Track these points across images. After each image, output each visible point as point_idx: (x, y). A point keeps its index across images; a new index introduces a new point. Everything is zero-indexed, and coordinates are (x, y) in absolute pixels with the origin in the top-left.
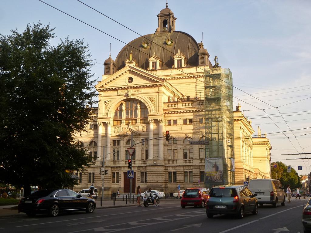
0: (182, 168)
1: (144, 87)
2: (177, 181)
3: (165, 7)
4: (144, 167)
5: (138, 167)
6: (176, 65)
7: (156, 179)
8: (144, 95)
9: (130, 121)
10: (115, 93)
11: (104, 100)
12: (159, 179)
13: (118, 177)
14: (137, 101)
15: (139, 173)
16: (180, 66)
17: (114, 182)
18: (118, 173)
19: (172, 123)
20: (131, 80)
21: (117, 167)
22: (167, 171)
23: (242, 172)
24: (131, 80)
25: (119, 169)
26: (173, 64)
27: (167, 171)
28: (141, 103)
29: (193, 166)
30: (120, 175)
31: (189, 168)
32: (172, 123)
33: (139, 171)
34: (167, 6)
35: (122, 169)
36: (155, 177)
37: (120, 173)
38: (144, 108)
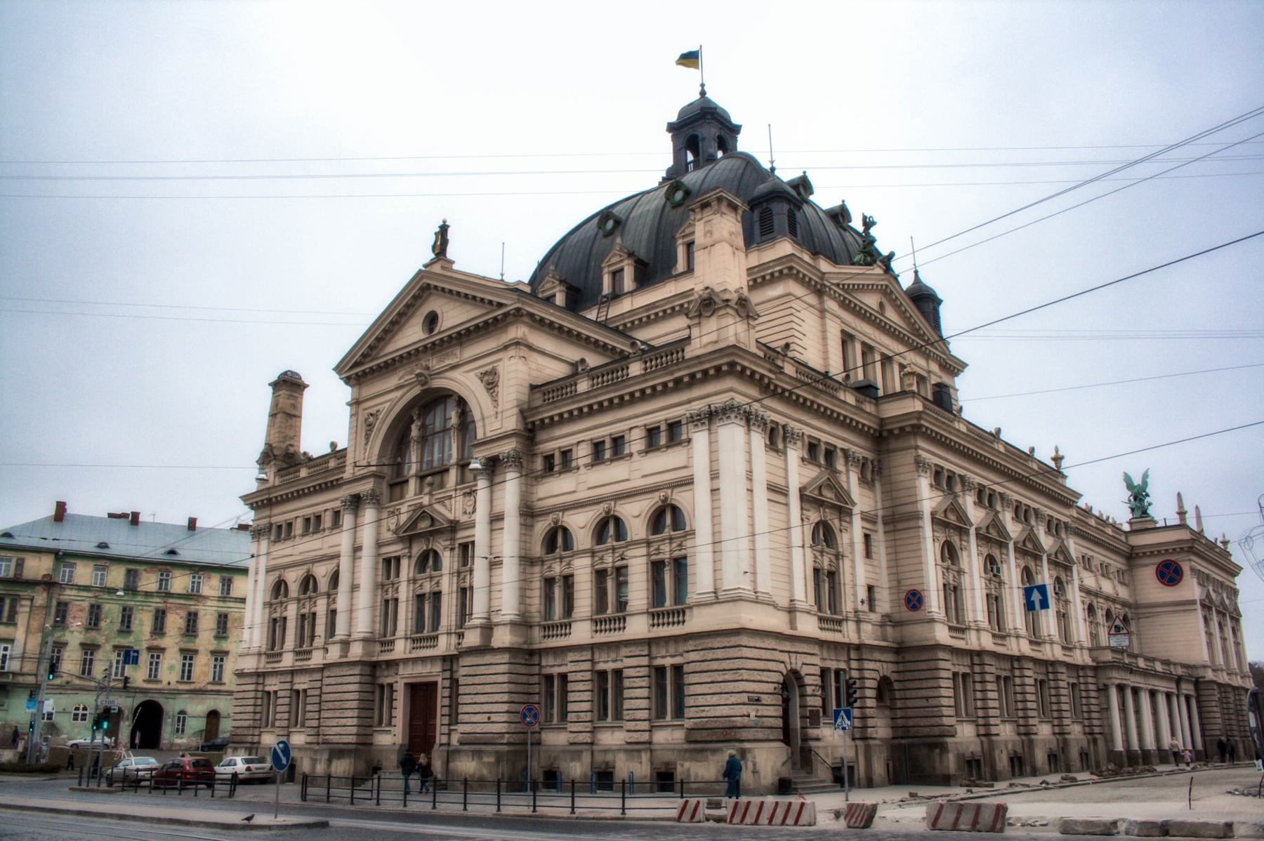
0: (587, 655)
2: (571, 717)
3: (698, 97)
5: (444, 658)
6: (681, 266)
10: (393, 381)
13: (392, 700)
15: (447, 683)
18: (391, 685)
19: (557, 459)
22: (536, 670)
23: (931, 665)
24: (432, 320)
25: (392, 671)
26: (673, 261)
27: (536, 670)
28: (462, 403)
31: (613, 656)
32: (557, 459)
34: (703, 93)
35: (402, 670)
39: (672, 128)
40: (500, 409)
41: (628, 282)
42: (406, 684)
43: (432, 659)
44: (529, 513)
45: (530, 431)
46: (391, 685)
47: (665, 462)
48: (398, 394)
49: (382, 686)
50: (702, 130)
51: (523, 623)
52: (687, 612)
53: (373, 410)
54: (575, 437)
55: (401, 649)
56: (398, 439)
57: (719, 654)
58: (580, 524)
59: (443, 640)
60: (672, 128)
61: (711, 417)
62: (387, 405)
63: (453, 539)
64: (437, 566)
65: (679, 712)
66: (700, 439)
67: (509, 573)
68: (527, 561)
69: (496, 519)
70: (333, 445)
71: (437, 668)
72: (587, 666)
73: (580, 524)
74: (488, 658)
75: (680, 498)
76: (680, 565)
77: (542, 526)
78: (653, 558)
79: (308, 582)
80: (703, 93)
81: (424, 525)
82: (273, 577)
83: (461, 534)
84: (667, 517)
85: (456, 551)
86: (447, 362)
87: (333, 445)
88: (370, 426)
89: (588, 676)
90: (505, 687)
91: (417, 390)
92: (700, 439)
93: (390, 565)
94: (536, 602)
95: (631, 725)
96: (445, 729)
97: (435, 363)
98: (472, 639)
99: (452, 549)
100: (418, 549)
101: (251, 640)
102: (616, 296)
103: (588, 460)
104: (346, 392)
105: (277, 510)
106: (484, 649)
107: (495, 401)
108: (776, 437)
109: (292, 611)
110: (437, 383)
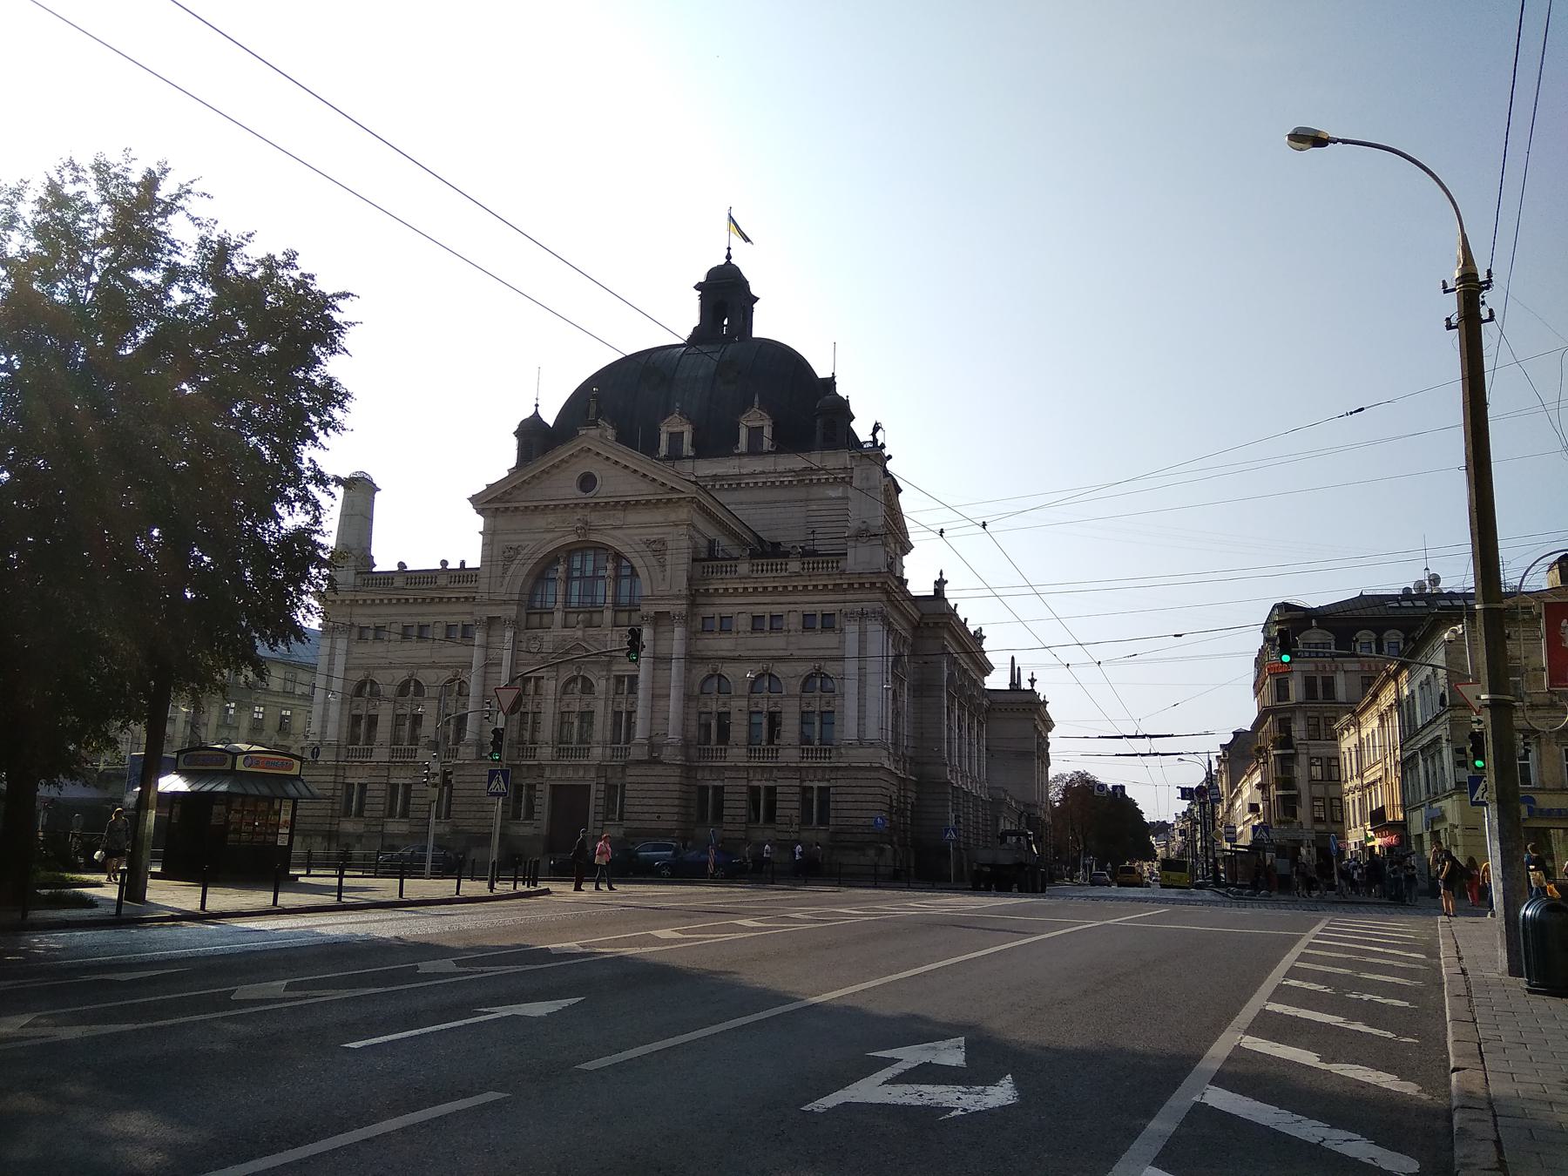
1: (627, 505)
7: (655, 809)
10: (540, 521)
12: (666, 809)
16: (754, 451)
18: (532, 787)
20: (587, 482)
24: (587, 482)
28: (618, 556)
29: (779, 769)
34: (729, 257)
35: (547, 773)
36: (651, 802)
39: (698, 287)
40: (668, 573)
41: (687, 449)
42: (553, 787)
44: (691, 658)
45: (695, 596)
46: (532, 787)
47: (822, 642)
48: (549, 536)
49: (519, 788)
50: (726, 294)
51: (686, 745)
52: (834, 753)
53: (515, 545)
54: (739, 610)
56: (541, 574)
57: (863, 783)
59: (597, 752)
60: (698, 287)
61: (863, 615)
63: (609, 670)
64: (588, 687)
65: (823, 820)
66: (852, 629)
67: (674, 705)
68: (688, 697)
69: (661, 660)
70: (444, 563)
72: (744, 782)
74: (658, 770)
75: (831, 668)
76: (827, 717)
77: (702, 671)
79: (410, 688)
80: (729, 257)
82: (359, 676)
84: (818, 680)
85: (612, 681)
87: (444, 563)
88: (511, 560)
89: (745, 789)
90: (676, 795)
91: (572, 538)
92: (852, 629)
94: (693, 730)
95: (780, 827)
96: (599, 824)
97: (594, 518)
98: (637, 753)
100: (565, 674)
101: (323, 733)
102: (675, 455)
104: (479, 522)
105: (357, 610)
106: (654, 761)
108: (890, 630)
109: (385, 713)
110: (595, 537)
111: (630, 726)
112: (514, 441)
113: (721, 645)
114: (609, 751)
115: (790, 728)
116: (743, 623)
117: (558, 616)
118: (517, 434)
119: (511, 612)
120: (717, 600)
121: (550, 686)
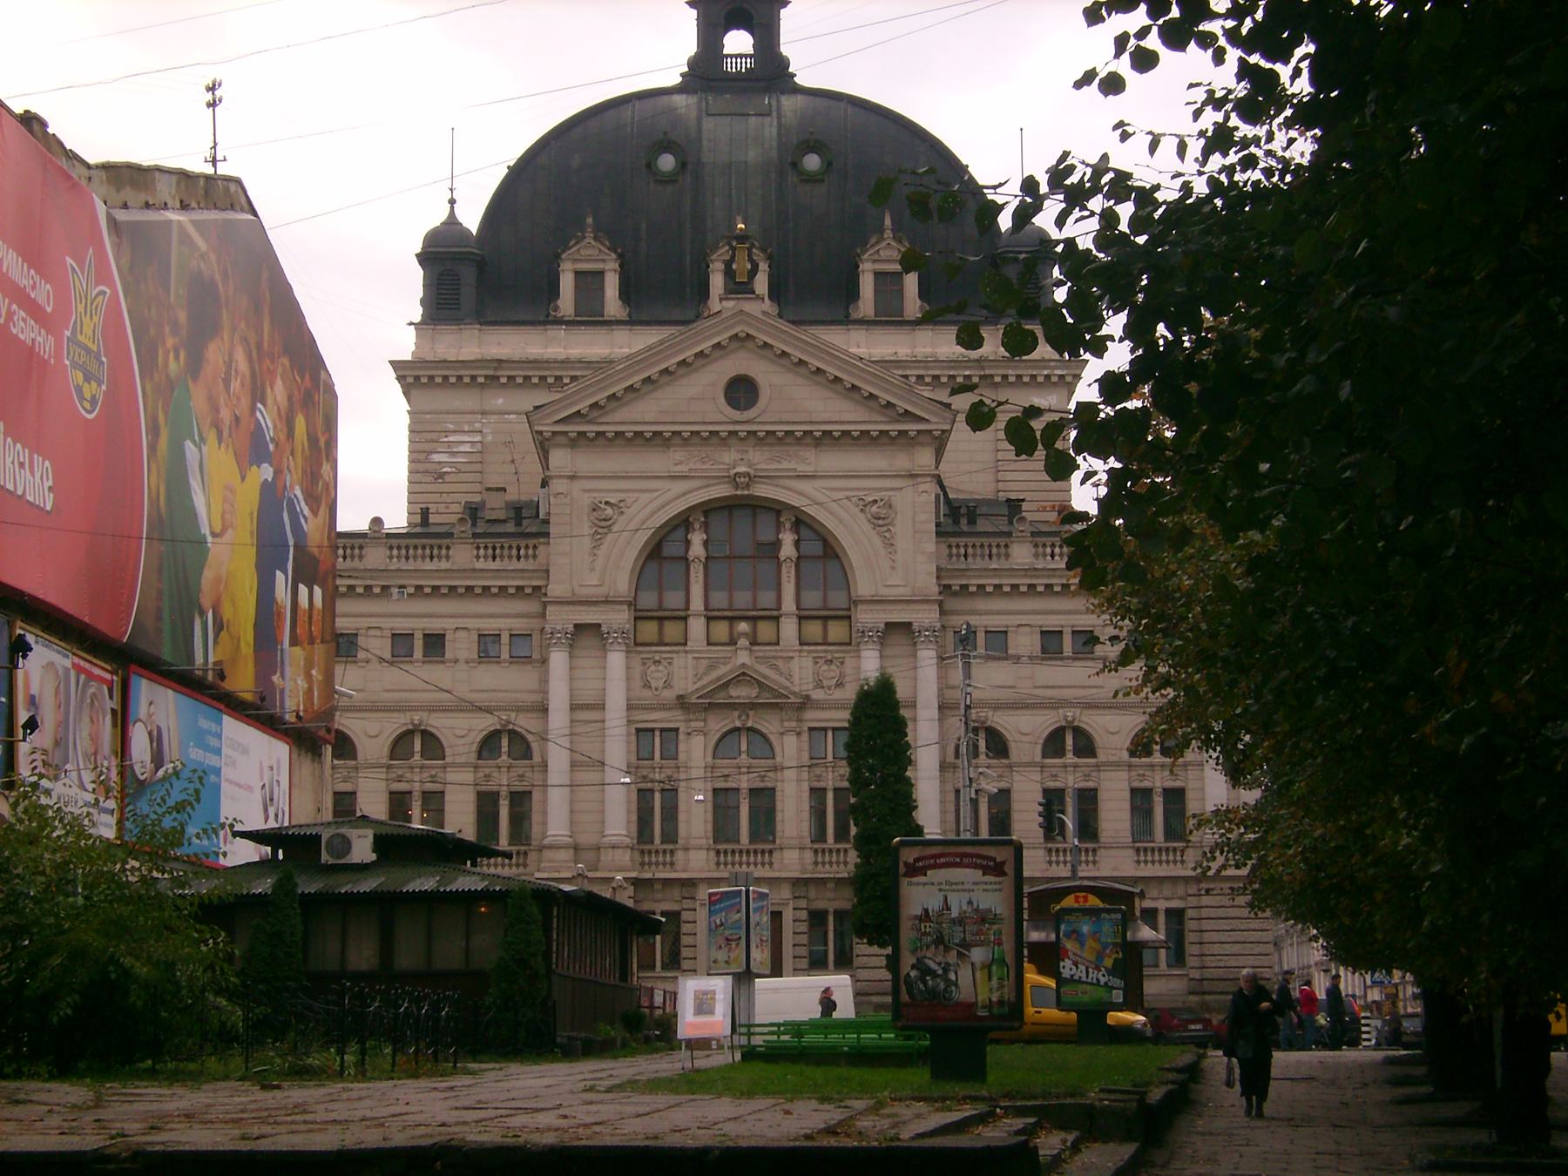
1: (826, 439)
4: (831, 885)
5: (796, 882)
8: (824, 489)
9: (743, 626)
10: (657, 461)
11: (586, 500)
14: (779, 513)
15: (804, 915)
17: (653, 967)
20: (741, 391)
21: (667, 882)
24: (741, 391)
28: (802, 522)
30: (685, 928)
33: (803, 903)
37: (685, 916)
38: (824, 552)
43: (772, 882)
55: (696, 861)
58: (1025, 730)
62: (646, 497)
71: (786, 893)
73: (1025, 730)
78: (1136, 784)
81: (741, 693)
83: (809, 715)
85: (805, 736)
86: (785, 465)
91: (722, 491)
93: (652, 741)
99: (799, 734)
103: (1037, 650)
107: (889, 544)
110: (762, 490)
111: (671, 814)
112: (418, 273)
113: (991, 678)
114: (809, 855)
115: (1115, 816)
116: (1025, 643)
117: (697, 626)
118: (424, 258)
119: (619, 618)
120: (982, 604)
121: (695, 751)
